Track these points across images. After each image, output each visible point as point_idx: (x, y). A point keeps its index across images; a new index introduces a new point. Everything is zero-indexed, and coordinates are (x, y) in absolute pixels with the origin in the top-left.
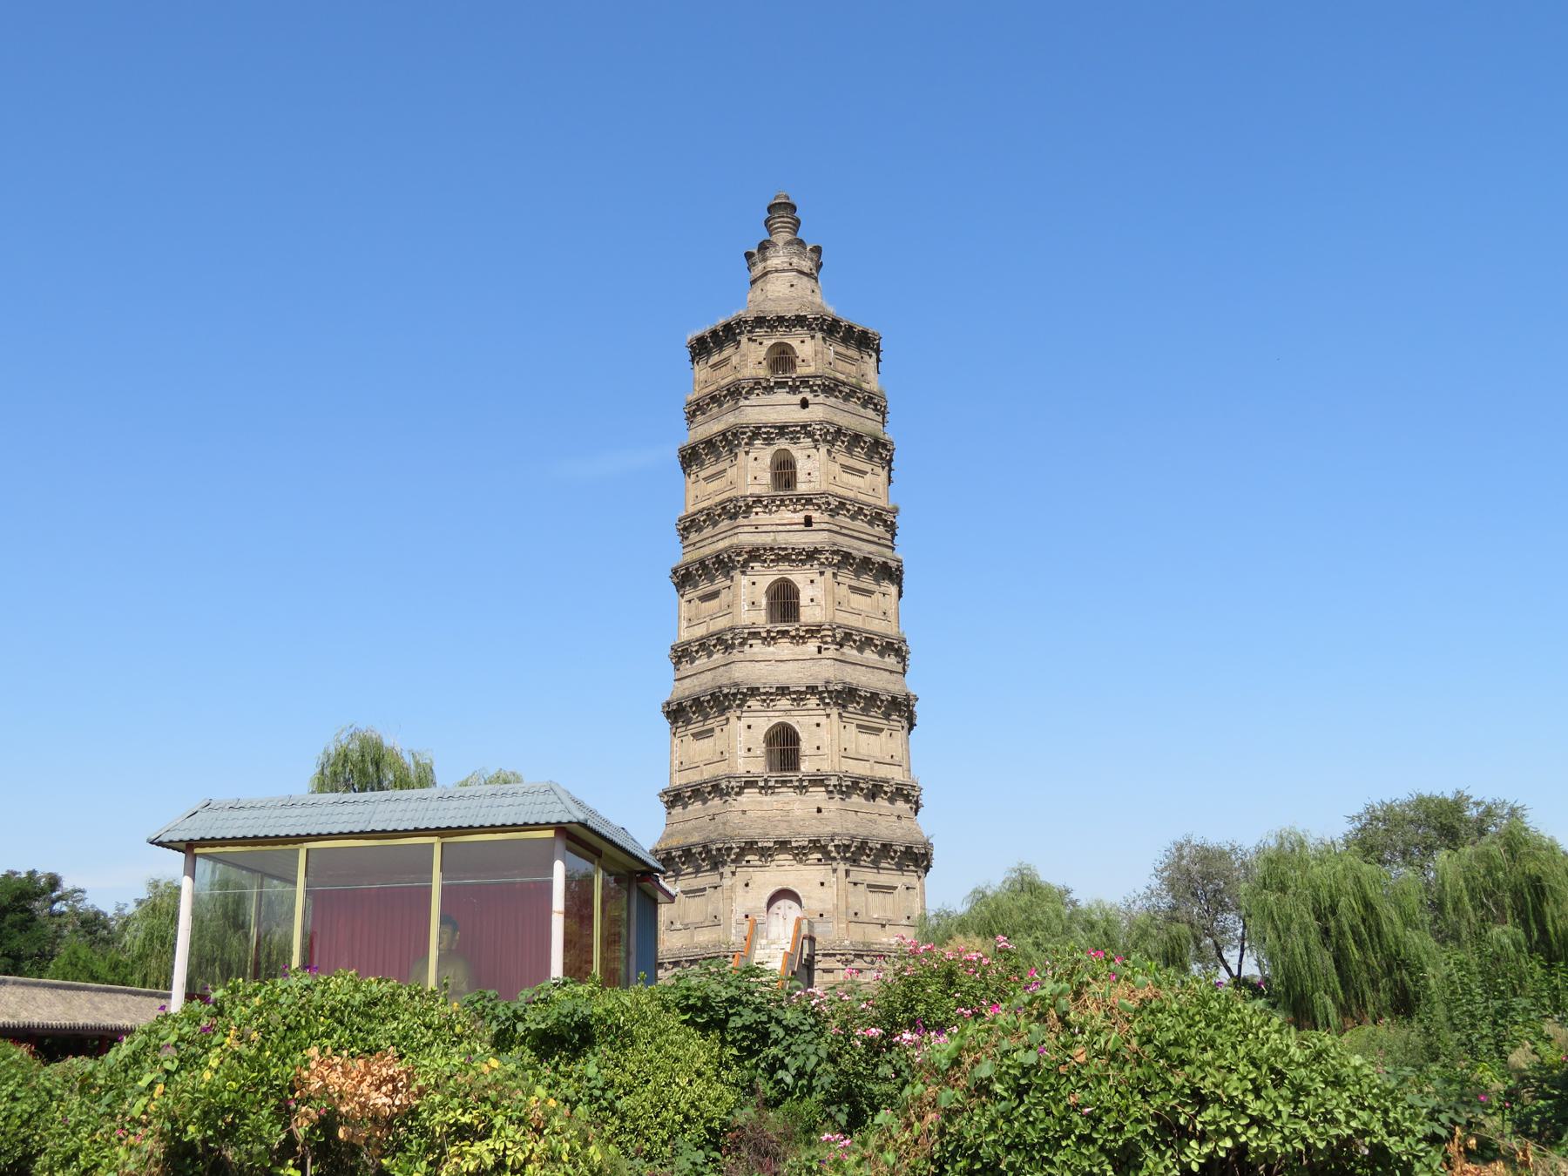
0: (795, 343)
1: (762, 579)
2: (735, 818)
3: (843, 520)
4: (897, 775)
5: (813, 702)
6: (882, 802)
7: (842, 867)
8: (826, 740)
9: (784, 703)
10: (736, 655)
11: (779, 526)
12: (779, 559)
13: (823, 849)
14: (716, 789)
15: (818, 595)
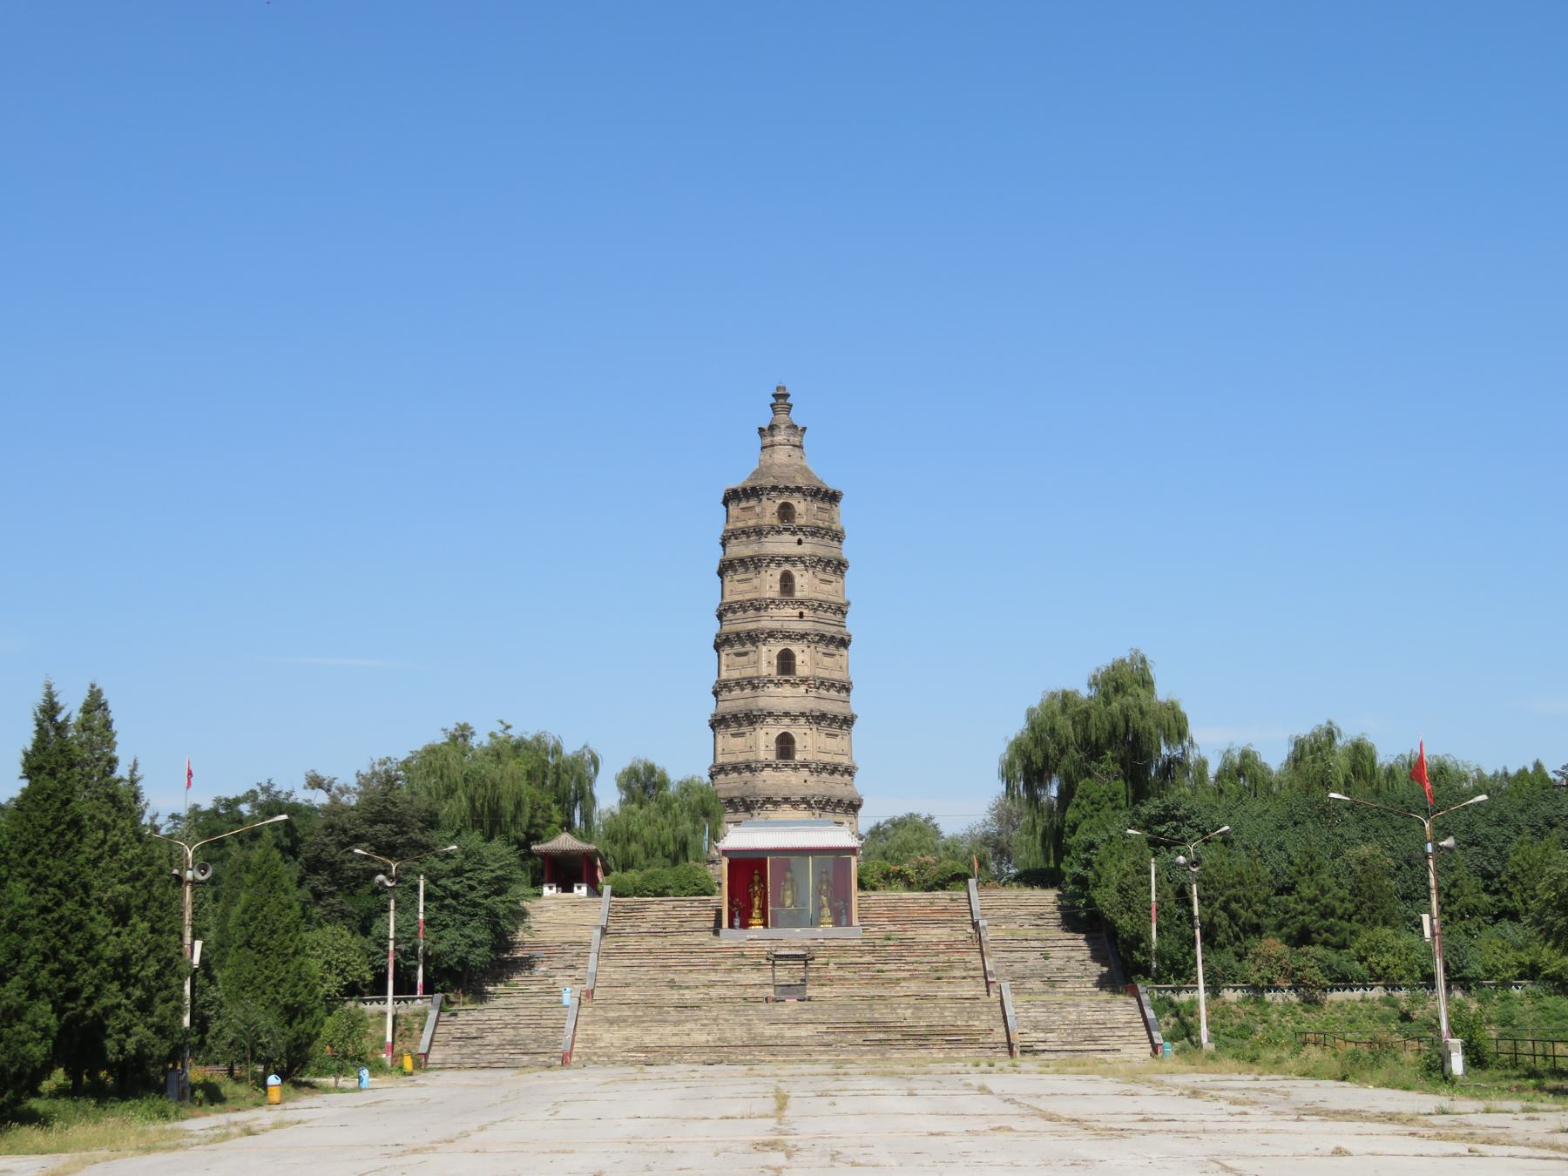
0: (794, 502)
1: (776, 648)
2: (760, 784)
3: (820, 613)
4: (845, 761)
5: (803, 721)
6: (837, 776)
7: (818, 812)
8: (809, 742)
9: (787, 721)
10: (759, 692)
11: (783, 617)
12: (785, 637)
13: (808, 803)
14: (748, 767)
15: (804, 658)
